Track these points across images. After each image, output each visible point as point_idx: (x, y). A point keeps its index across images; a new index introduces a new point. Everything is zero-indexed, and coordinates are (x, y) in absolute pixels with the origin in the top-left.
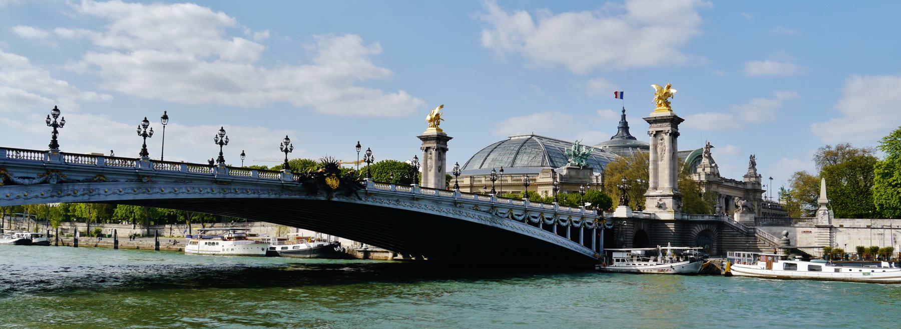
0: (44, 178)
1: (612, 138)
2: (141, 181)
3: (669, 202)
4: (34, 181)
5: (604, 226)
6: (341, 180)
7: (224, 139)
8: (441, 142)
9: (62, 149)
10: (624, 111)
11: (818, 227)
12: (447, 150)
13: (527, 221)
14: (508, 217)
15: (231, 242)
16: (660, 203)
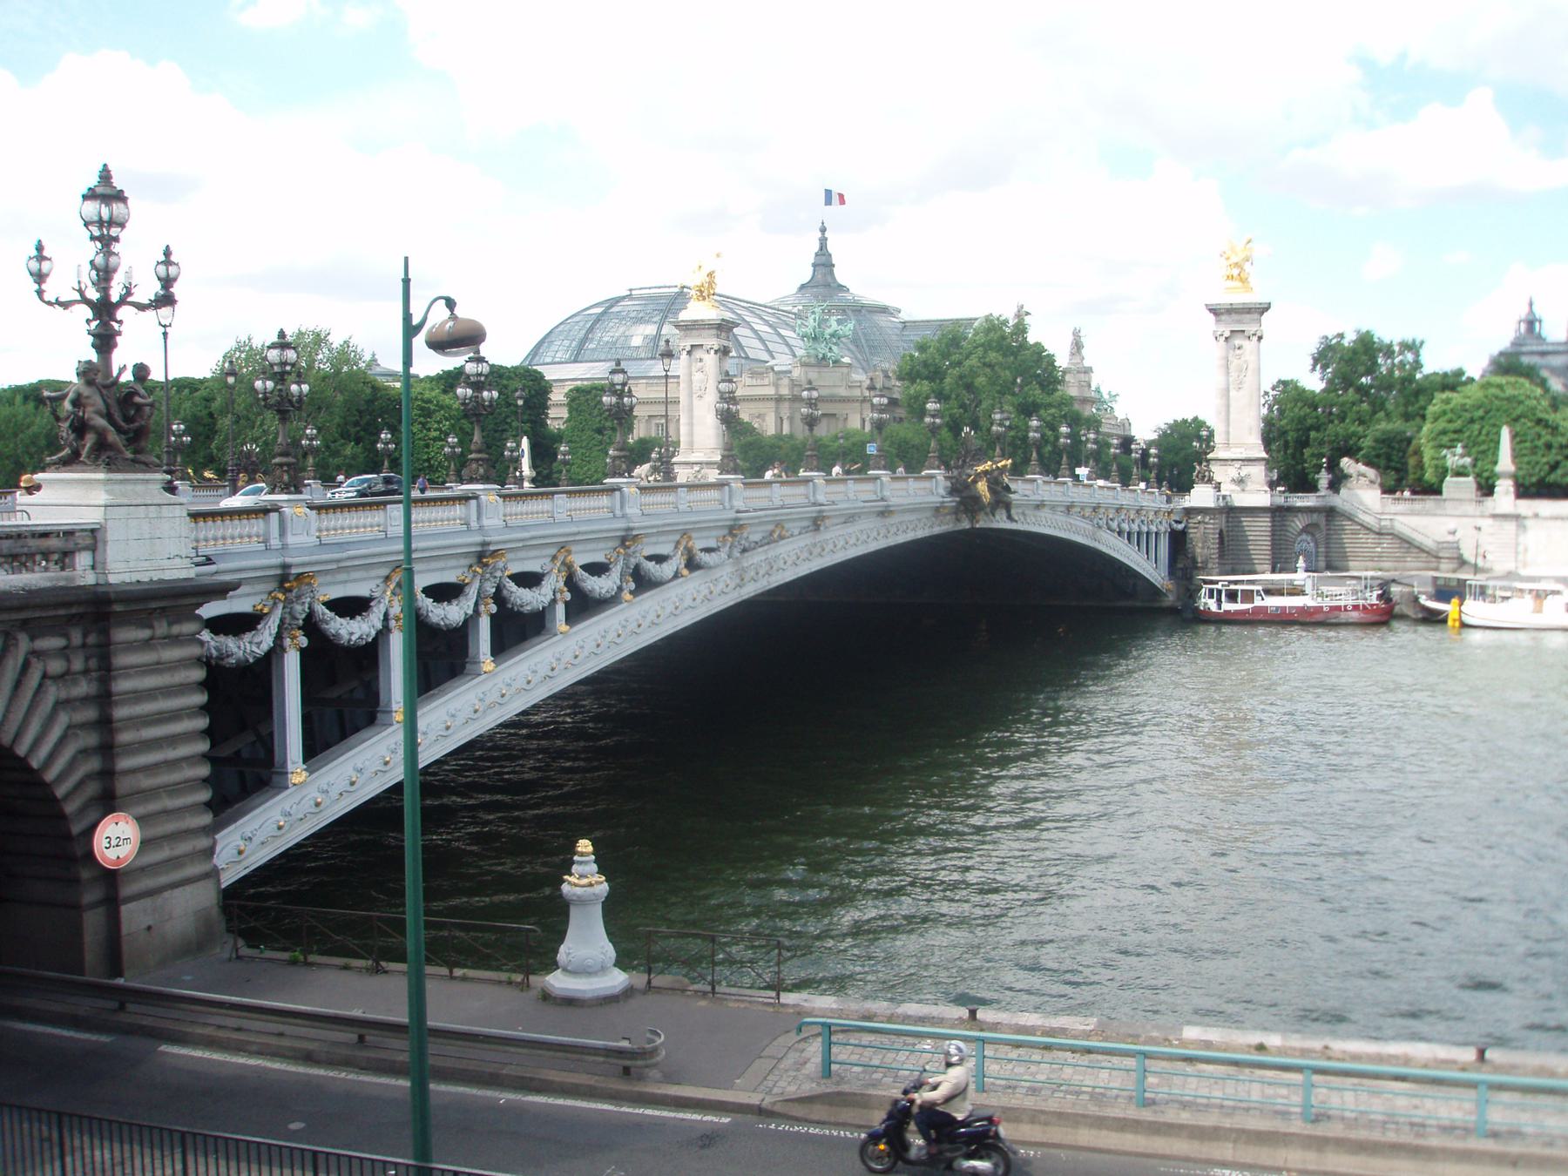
0: (728, 545)
1: (803, 287)
3: (1258, 473)
4: (723, 554)
8: (723, 334)
10: (823, 230)
11: (1494, 516)
16: (1242, 474)
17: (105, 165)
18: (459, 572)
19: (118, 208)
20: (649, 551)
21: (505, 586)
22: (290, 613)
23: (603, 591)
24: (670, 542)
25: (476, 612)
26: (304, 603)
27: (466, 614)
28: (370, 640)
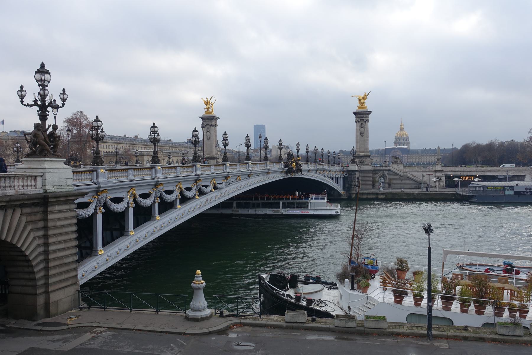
17: (43, 62)
18: (149, 190)
19: (47, 76)
20: (203, 184)
21: (162, 194)
22: (99, 202)
23: (190, 196)
24: (209, 181)
25: (155, 202)
26: (103, 199)
27: (151, 202)
28: (123, 210)
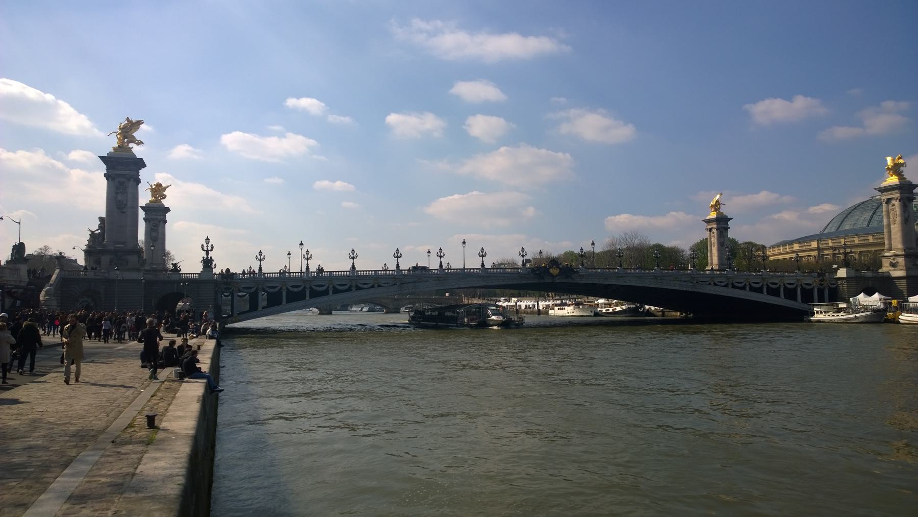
2: (440, 280)
3: (901, 261)
4: (390, 284)
5: (828, 286)
6: (560, 269)
7: (484, 254)
8: (721, 223)
9: (401, 268)
12: (729, 228)
13: (730, 286)
14: (710, 284)
15: (572, 307)
16: (894, 262)
